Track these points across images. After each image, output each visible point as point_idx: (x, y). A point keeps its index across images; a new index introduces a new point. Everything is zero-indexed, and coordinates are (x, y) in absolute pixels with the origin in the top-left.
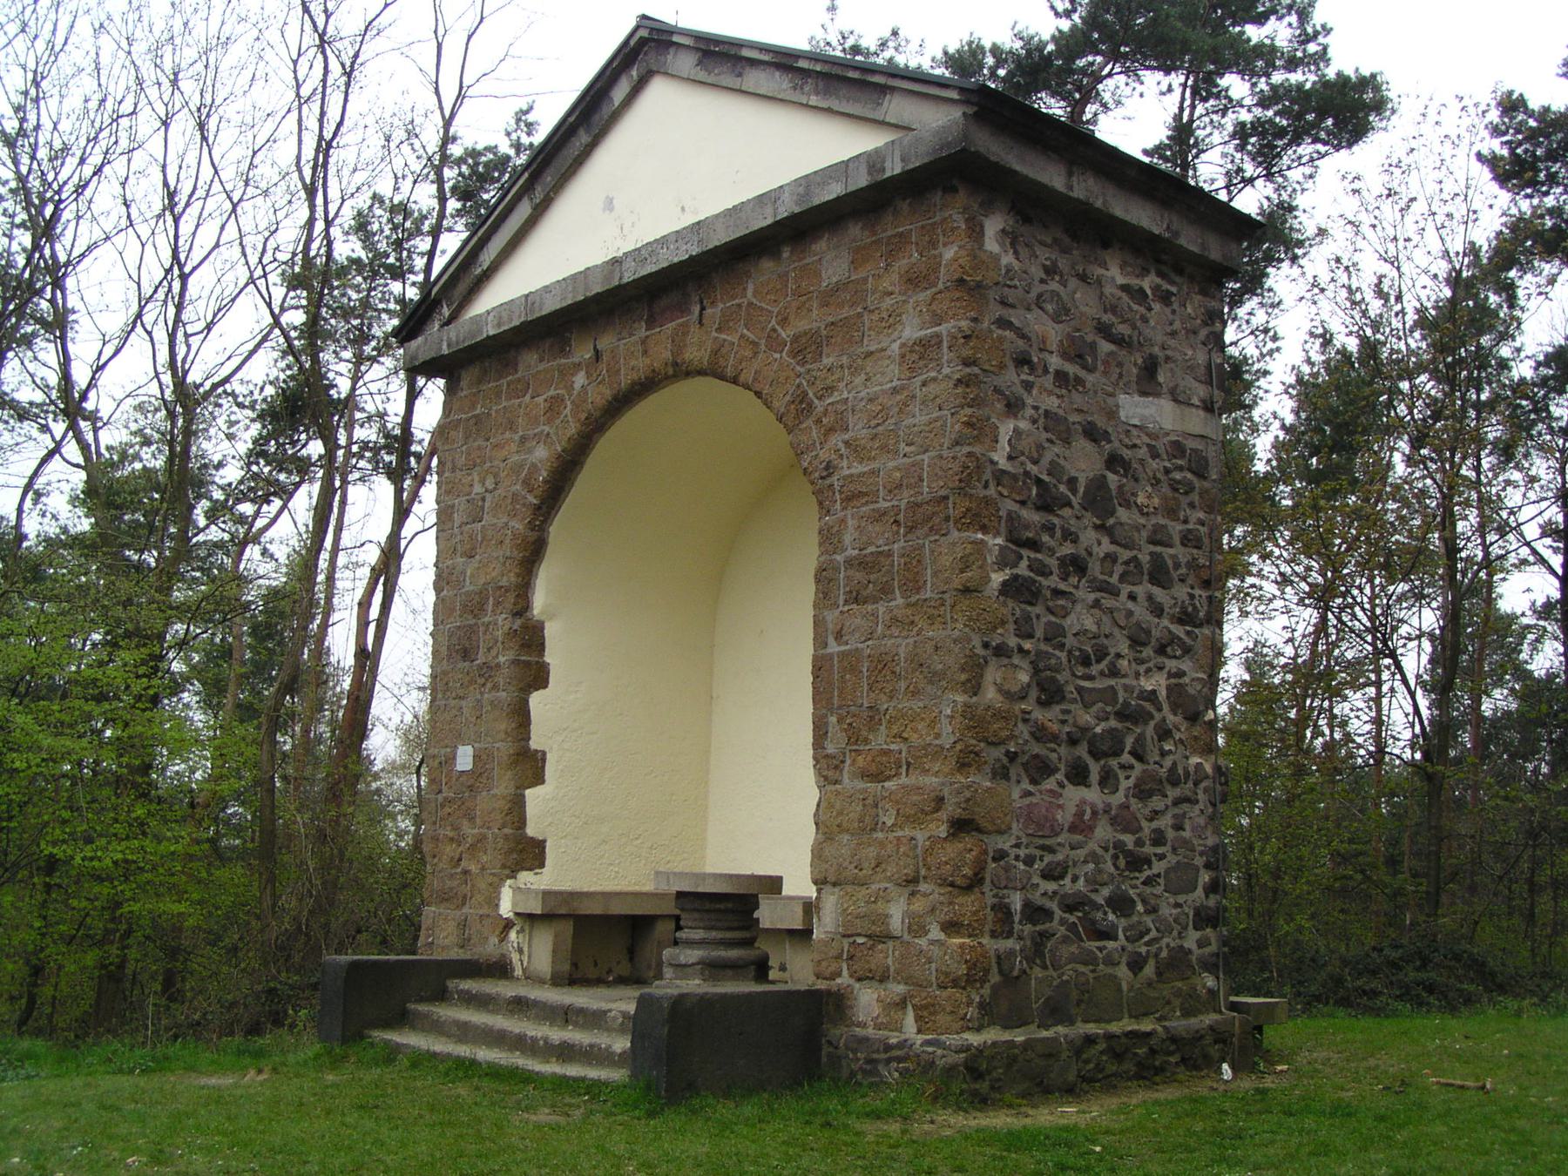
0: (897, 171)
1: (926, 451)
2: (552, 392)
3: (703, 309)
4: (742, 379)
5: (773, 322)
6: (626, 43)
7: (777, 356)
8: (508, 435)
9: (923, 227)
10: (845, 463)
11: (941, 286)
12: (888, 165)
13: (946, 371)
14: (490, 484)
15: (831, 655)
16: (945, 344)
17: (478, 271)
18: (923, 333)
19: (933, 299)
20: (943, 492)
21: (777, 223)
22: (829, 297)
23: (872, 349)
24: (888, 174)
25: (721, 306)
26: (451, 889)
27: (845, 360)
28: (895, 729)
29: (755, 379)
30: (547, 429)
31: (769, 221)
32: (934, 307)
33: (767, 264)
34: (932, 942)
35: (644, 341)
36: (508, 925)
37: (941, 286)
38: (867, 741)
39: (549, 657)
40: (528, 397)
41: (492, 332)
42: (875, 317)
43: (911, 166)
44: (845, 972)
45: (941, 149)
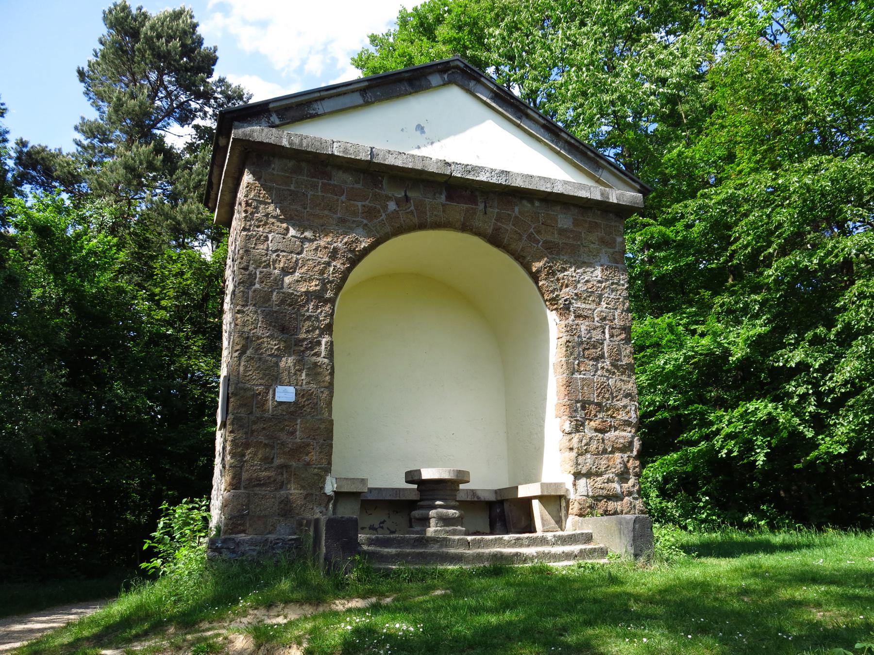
0: (615, 201)
2: (367, 203)
3: (485, 207)
5: (532, 230)
8: (326, 212)
22: (562, 232)
25: (497, 210)
26: (269, 478)
27: (572, 260)
30: (365, 221)
31: (549, 190)
33: (525, 203)
35: (443, 205)
36: (329, 498)
37: (617, 250)
40: (343, 198)
42: (586, 249)
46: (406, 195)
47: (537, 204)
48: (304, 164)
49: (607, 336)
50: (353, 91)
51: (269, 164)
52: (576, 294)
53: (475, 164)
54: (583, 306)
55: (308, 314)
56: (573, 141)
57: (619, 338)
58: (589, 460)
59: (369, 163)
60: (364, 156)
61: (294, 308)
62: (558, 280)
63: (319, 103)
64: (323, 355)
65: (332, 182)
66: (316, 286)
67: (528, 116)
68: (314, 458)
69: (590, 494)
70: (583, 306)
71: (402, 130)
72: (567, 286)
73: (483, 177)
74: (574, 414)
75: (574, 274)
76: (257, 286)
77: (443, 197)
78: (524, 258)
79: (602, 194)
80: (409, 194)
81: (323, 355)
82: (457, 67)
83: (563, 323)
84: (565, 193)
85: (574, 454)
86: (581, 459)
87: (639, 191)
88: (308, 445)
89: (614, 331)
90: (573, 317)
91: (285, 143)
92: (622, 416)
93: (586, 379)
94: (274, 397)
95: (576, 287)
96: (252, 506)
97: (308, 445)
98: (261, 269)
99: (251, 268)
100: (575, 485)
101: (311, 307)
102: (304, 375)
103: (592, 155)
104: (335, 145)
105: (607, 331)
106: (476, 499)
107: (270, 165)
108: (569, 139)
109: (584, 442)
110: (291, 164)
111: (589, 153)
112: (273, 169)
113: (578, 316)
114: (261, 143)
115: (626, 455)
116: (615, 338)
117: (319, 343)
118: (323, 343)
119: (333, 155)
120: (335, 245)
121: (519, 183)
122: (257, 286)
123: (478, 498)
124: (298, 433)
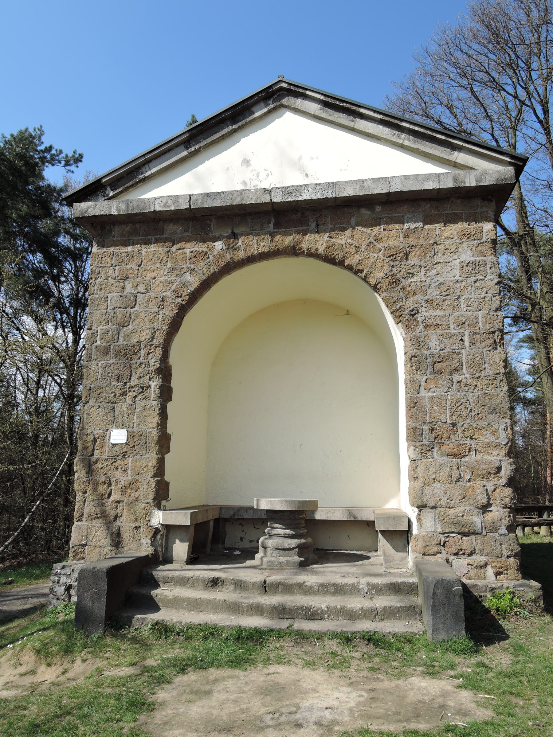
0: (474, 184)
1: (480, 310)
4: (347, 263)
6: (270, 87)
7: (376, 255)
9: (470, 213)
10: (424, 309)
11: (484, 240)
12: (467, 180)
13: (489, 277)
14: (141, 288)
15: (424, 398)
16: (488, 266)
17: (142, 176)
18: (474, 259)
19: (478, 245)
20: (492, 330)
21: (389, 194)
23: (441, 261)
24: (467, 184)
28: (467, 434)
29: (358, 264)
31: (385, 191)
32: (480, 248)
34: (501, 535)
38: (449, 438)
39: (172, 385)
41: (158, 209)
43: (481, 184)
44: (443, 551)
45: (502, 180)
46: (233, 232)
47: (378, 209)
48: (138, 226)
49: (467, 343)
50: (177, 145)
51: (110, 231)
52: (427, 301)
53: (296, 184)
54: (436, 313)
55: (139, 361)
56: (416, 128)
57: (483, 344)
58: (438, 491)
59: (189, 209)
60: (184, 205)
61: (128, 358)
62: (403, 288)
63: (146, 166)
64: (152, 398)
65: (164, 236)
66: (146, 335)
67: (362, 117)
68: (142, 494)
69: (439, 530)
70: (436, 313)
71: (228, 169)
72: (415, 293)
73: (306, 196)
74: (420, 439)
75: (424, 279)
76: (99, 343)
77: (271, 225)
78: (361, 271)
79: (456, 180)
80: (236, 231)
81: (152, 398)
82: (282, 89)
83: (409, 336)
84: (406, 189)
85: (419, 483)
86: (427, 490)
87: (510, 164)
88: (137, 481)
89: (477, 337)
90: (421, 327)
91: (115, 212)
92: (487, 437)
93: (436, 397)
94: (109, 440)
95: (425, 293)
96: (90, 537)
97: (137, 481)
98: (101, 327)
99: (94, 328)
100: (419, 519)
101: (142, 355)
102: (135, 418)
103: (443, 137)
104: (157, 202)
105: (466, 338)
106: (352, 519)
107: (111, 233)
108: (412, 127)
109: (432, 469)
110: (128, 228)
111: (439, 136)
112: (114, 236)
113: (427, 326)
114: (95, 216)
115: (491, 483)
116: (478, 345)
117: (149, 387)
118: (153, 387)
119: (155, 211)
120: (164, 294)
121: (349, 192)
122: (99, 343)
123: (355, 517)
124: (129, 471)
